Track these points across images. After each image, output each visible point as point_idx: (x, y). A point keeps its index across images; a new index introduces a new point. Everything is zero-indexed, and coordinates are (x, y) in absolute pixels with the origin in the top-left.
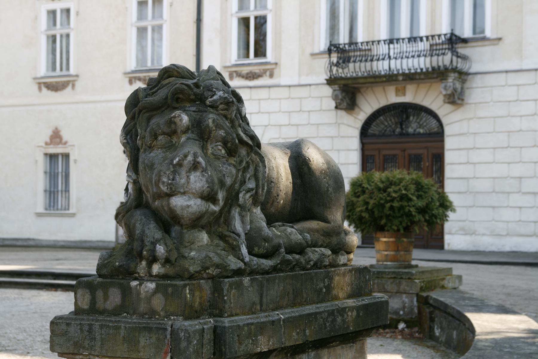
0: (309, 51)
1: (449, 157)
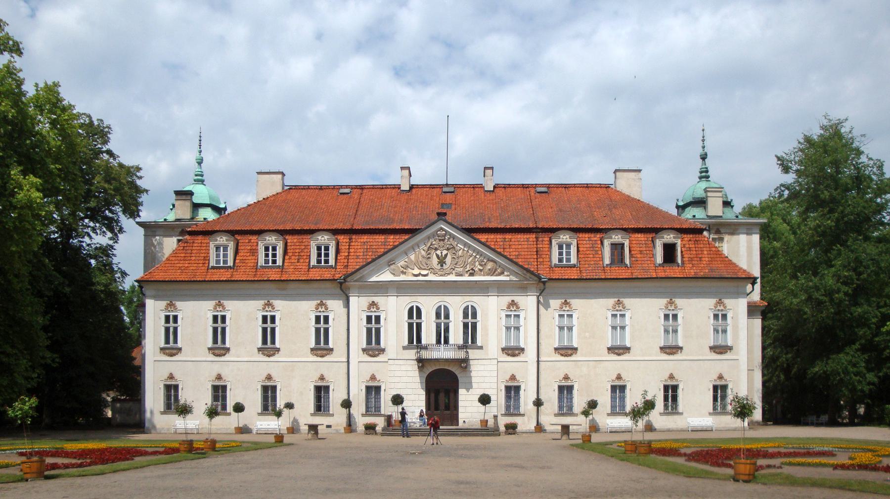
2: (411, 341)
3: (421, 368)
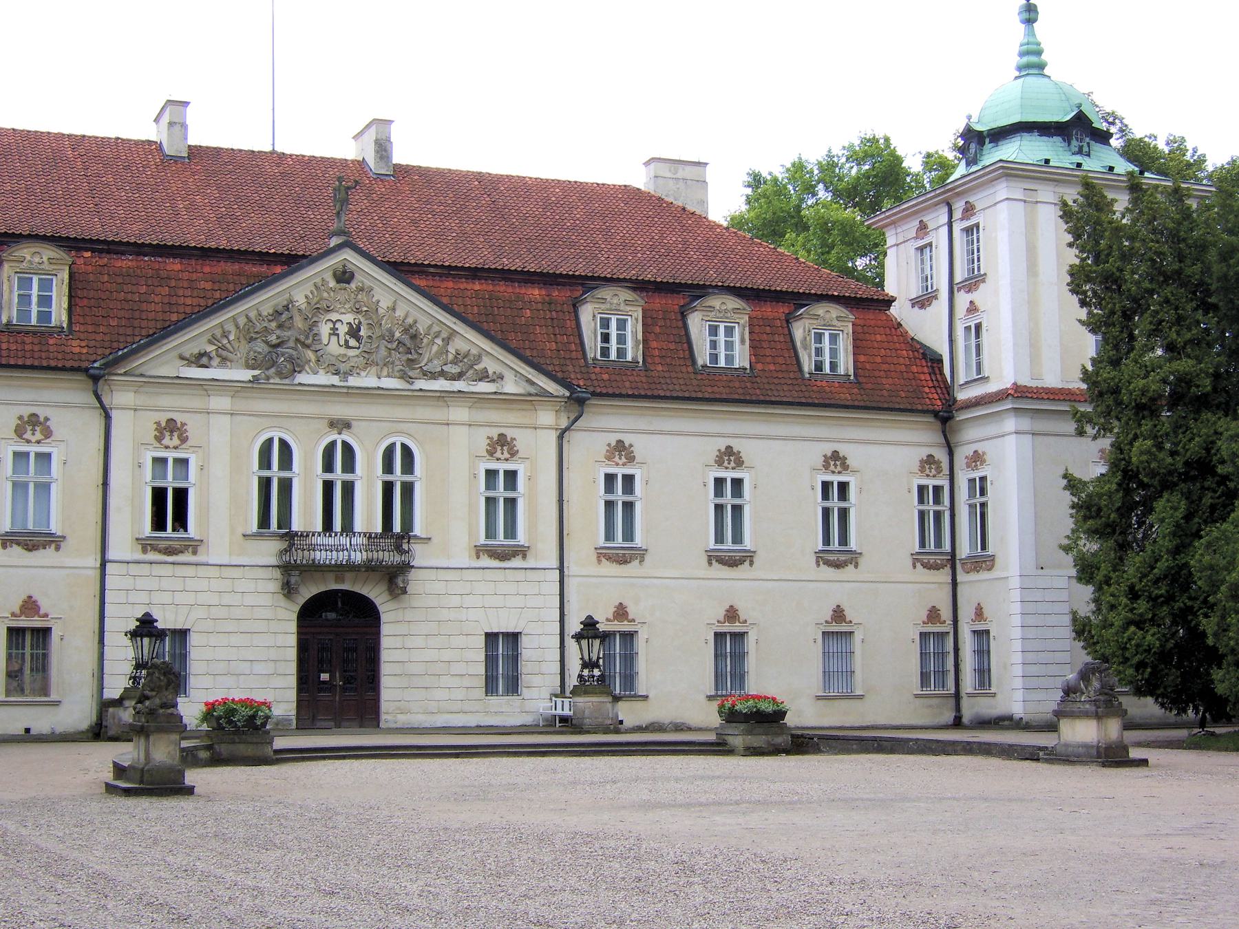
0: (240, 531)
1: (385, 642)
2: (264, 521)
3: (288, 590)
